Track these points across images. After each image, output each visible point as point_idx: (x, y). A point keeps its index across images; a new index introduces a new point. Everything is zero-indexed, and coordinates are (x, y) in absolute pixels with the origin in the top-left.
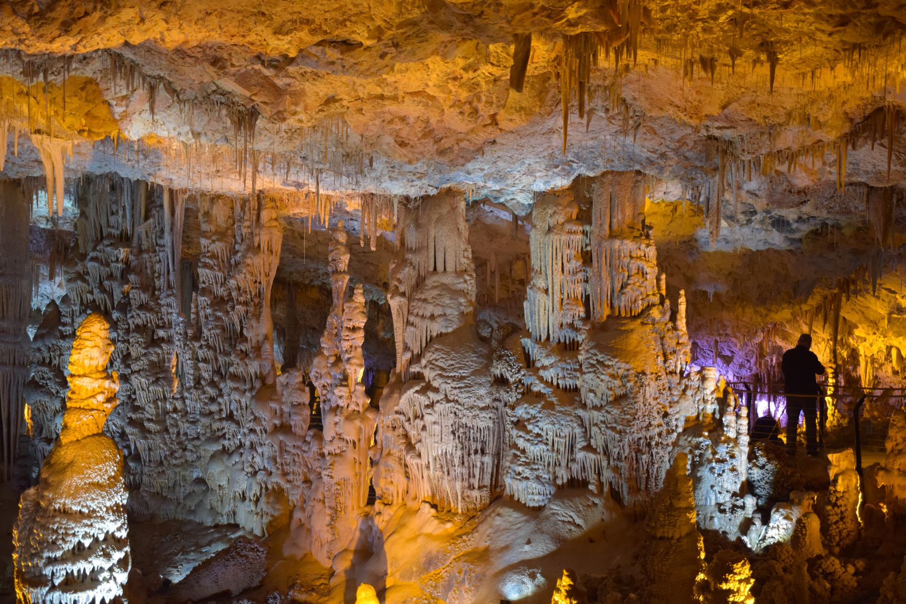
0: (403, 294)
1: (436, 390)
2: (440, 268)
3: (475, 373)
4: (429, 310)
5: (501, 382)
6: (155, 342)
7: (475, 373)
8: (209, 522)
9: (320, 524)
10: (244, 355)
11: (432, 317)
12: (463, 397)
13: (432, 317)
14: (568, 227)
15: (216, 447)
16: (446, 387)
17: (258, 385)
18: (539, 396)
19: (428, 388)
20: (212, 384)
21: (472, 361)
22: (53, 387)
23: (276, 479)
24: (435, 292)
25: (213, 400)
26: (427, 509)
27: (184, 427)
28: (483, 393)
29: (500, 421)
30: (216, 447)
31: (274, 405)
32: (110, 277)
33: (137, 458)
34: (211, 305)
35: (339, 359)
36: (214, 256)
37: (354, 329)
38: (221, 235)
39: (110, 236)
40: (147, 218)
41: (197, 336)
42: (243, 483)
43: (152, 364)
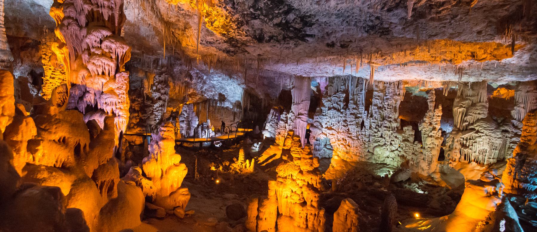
0: (465, 107)
1: (483, 133)
2: (482, 101)
3: (495, 129)
4: (478, 112)
5: (506, 131)
7: (495, 129)
8: (374, 162)
9: (424, 165)
10: (390, 122)
11: (479, 114)
12: (493, 135)
13: (479, 114)
14: (534, 91)
15: (377, 144)
16: (486, 132)
17: (396, 129)
19: (478, 132)
20: (376, 128)
21: (493, 126)
22: (320, 127)
23: (403, 153)
24: (481, 107)
25: (376, 132)
26: (474, 164)
27: (365, 138)
28: (499, 134)
30: (377, 144)
31: (403, 135)
32: (340, 101)
34: (377, 109)
35: (431, 124)
36: (379, 96)
37: (439, 116)
38: (382, 91)
39: (341, 91)
40: (357, 87)
41: (371, 116)
42: (387, 153)
43: (357, 123)
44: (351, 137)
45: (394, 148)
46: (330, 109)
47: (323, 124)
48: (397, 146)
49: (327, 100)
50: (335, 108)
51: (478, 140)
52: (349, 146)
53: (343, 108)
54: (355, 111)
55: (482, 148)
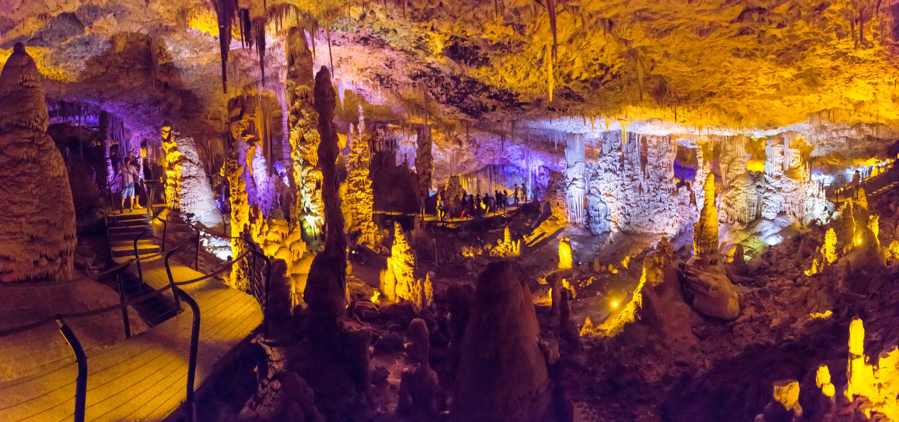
6: (633, 180)
16: (743, 189)
18: (771, 190)
19: (737, 189)
22: (597, 194)
27: (644, 205)
28: (754, 190)
29: (759, 198)
33: (629, 214)
41: (648, 177)
44: (629, 205)
45: (673, 214)
46: (606, 171)
47: (601, 190)
48: (675, 210)
49: (601, 160)
50: (611, 170)
51: (737, 198)
52: (629, 214)
53: (620, 170)
54: (630, 172)
55: (741, 206)
